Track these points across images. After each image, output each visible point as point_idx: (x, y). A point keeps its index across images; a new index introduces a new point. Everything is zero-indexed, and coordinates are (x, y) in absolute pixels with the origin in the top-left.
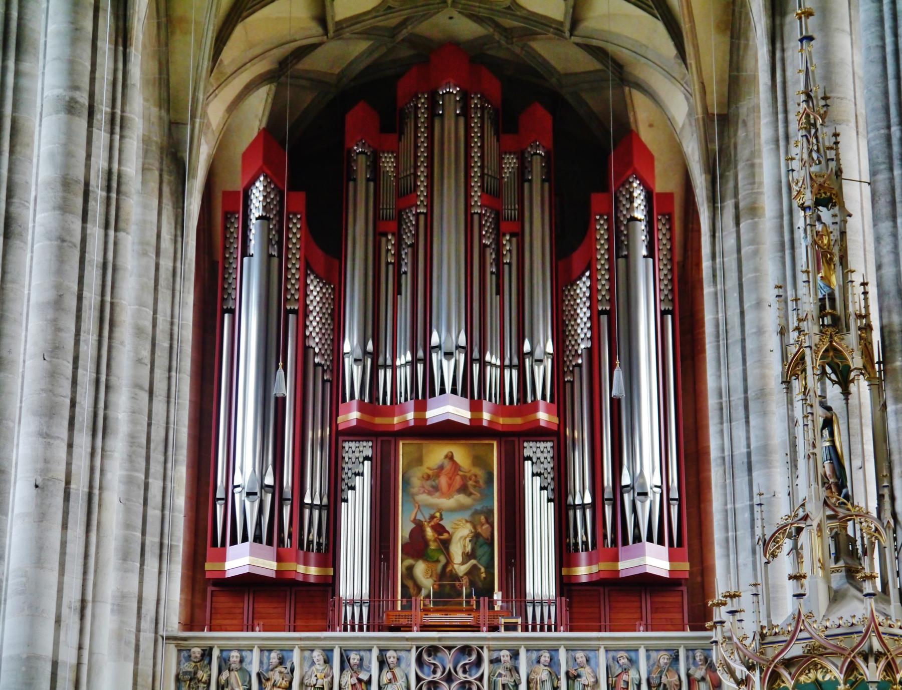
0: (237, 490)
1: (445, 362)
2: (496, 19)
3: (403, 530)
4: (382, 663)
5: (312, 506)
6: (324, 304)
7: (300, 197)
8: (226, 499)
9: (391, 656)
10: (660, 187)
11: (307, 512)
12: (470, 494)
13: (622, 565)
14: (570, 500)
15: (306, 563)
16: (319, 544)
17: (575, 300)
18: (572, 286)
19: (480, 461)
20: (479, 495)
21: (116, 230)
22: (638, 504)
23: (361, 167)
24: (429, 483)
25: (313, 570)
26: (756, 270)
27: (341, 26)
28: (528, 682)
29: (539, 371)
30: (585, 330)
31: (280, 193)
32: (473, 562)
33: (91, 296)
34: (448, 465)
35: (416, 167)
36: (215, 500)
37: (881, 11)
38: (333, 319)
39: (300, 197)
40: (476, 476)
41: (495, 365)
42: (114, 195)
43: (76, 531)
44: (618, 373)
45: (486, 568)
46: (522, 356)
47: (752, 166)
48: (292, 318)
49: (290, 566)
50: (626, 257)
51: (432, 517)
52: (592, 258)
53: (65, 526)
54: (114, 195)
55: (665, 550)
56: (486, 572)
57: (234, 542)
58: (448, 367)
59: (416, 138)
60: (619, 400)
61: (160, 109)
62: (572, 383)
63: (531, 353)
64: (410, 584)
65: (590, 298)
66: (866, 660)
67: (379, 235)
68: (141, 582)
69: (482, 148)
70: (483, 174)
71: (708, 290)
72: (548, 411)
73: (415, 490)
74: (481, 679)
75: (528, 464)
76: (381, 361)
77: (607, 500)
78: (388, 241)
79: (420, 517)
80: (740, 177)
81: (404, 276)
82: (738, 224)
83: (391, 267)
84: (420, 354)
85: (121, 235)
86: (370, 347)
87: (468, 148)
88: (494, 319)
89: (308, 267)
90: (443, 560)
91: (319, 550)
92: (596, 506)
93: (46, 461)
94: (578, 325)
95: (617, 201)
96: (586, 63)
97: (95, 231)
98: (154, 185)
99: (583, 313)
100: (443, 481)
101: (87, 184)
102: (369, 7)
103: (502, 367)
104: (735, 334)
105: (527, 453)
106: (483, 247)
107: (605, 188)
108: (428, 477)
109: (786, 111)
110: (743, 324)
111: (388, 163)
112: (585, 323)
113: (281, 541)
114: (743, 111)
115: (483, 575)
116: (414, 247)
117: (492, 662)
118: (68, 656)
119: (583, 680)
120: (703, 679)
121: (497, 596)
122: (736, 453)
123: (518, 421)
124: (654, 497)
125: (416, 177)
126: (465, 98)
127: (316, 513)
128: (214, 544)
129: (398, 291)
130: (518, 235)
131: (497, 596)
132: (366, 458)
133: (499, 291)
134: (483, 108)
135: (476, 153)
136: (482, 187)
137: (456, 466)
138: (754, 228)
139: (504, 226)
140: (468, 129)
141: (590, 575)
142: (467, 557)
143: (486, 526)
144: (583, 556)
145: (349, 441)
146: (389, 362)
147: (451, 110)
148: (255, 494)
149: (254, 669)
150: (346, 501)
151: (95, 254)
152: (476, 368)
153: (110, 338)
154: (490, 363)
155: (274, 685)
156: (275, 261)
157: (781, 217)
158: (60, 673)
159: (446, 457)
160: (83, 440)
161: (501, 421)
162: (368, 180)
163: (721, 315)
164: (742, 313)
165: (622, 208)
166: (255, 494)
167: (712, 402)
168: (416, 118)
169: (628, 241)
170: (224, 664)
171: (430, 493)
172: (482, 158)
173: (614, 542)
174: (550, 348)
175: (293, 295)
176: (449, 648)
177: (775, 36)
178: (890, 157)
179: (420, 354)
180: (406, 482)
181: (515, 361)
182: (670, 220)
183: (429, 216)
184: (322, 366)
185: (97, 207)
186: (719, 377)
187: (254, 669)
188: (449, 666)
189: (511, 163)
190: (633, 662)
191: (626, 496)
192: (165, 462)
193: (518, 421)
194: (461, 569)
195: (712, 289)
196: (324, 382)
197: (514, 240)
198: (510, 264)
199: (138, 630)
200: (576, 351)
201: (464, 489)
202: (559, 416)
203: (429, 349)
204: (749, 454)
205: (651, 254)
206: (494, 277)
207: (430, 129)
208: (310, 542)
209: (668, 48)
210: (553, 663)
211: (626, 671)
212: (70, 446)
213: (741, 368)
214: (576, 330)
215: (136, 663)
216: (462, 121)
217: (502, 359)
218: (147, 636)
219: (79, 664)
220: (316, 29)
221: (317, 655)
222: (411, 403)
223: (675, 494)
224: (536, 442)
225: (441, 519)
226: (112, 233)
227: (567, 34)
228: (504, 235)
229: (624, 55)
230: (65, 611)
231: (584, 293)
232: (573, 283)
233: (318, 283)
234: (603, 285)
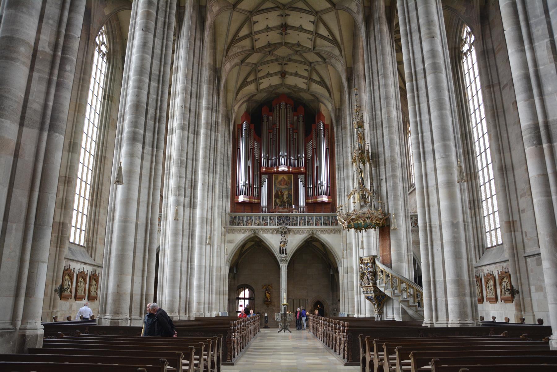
3: (274, 193)
4: (270, 219)
5: (256, 188)
7: (253, 125)
9: (272, 218)
10: (326, 123)
11: (255, 189)
12: (288, 185)
15: (255, 199)
19: (290, 178)
21: (217, 133)
22: (322, 187)
23: (265, 119)
25: (256, 201)
26: (346, 140)
27: (261, 90)
28: (300, 223)
29: (302, 160)
31: (249, 125)
33: (212, 146)
34: (283, 180)
36: (236, 187)
37: (371, 89)
39: (253, 125)
42: (217, 126)
43: (210, 193)
44: (318, 161)
46: (298, 157)
47: (345, 119)
49: (251, 200)
51: (280, 190)
53: (208, 192)
54: (217, 126)
55: (327, 196)
57: (240, 195)
58: (283, 160)
59: (276, 113)
60: (318, 166)
63: (300, 157)
64: (275, 203)
66: (367, 219)
68: (222, 203)
69: (290, 115)
71: (336, 144)
72: (303, 169)
73: (276, 185)
74: (290, 222)
76: (269, 158)
80: (342, 121)
82: (342, 131)
84: (277, 157)
85: (218, 134)
86: (267, 155)
89: (254, 139)
90: (282, 199)
93: (204, 179)
95: (317, 126)
96: (311, 98)
97: (213, 133)
98: (224, 123)
99: (310, 148)
100: (282, 183)
101: (211, 124)
103: (294, 160)
104: (341, 153)
105: (299, 177)
106: (290, 135)
107: (315, 123)
109: (352, 108)
110: (343, 151)
111: (271, 118)
113: (250, 195)
114: (343, 107)
116: (276, 135)
117: (292, 219)
118: (209, 217)
119: (310, 223)
120: (334, 222)
121: (294, 206)
123: (297, 170)
124: (325, 186)
126: (286, 104)
127: (257, 189)
128: (236, 195)
129: (273, 144)
130: (297, 133)
131: (294, 206)
134: (290, 107)
135: (288, 116)
136: (290, 123)
137: (285, 180)
138: (345, 132)
141: (312, 202)
142: (287, 198)
144: (310, 198)
147: (283, 107)
149: (245, 220)
151: (213, 138)
152: (289, 160)
153: (216, 154)
155: (249, 223)
156: (248, 138)
157: (351, 129)
158: (208, 221)
160: (211, 175)
161: (294, 170)
164: (343, 149)
167: (336, 167)
170: (239, 219)
171: (279, 185)
172: (290, 117)
173: (317, 195)
174: (304, 156)
176: (284, 216)
177: (349, 93)
178: (373, 118)
179: (277, 157)
181: (297, 158)
182: (328, 129)
183: (279, 129)
185: (213, 128)
186: (338, 162)
187: (245, 220)
188: (284, 220)
189: (296, 118)
190: (321, 219)
191: (319, 186)
192: (227, 179)
193: (297, 170)
194: (286, 200)
199: (222, 212)
201: (286, 184)
204: (344, 177)
205: (324, 136)
207: (279, 111)
208: (255, 195)
209: (327, 95)
210: (305, 219)
211: (319, 221)
212: (209, 176)
215: (222, 218)
216: (286, 109)
217: (294, 158)
218: (224, 214)
219: (211, 219)
220: (256, 91)
221: (257, 218)
222: (276, 167)
226: (216, 133)
227: (307, 91)
229: (319, 96)
230: (208, 208)
234: (314, 143)
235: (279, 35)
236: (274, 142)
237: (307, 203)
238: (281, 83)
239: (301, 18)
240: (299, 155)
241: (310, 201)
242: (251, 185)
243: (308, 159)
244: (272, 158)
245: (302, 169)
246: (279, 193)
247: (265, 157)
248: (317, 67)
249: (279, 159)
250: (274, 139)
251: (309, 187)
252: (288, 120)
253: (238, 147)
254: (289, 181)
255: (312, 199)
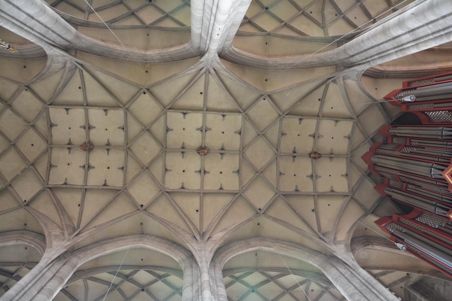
10: (401, 87)
18: (430, 119)
52: (418, 111)
61: (318, 256)
88: (431, 151)
89: (413, 219)
122: (411, 39)
139: (408, 144)
163: (376, 57)
195: (371, 62)
213: (385, 44)
234: (432, 106)
235: (225, 158)
238: (345, 159)
239: (184, 129)
248: (285, 106)
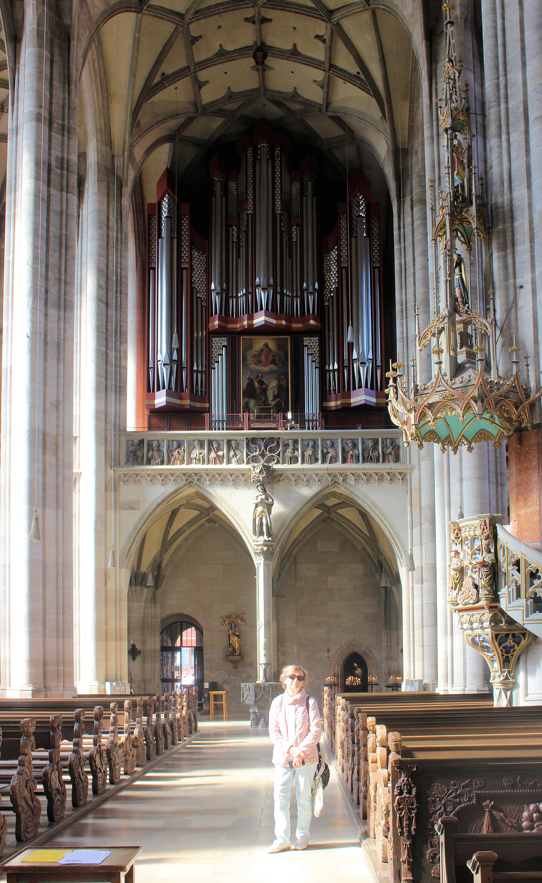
0: (159, 363)
1: (262, 294)
2: (288, 104)
3: (243, 384)
5: (197, 371)
6: (201, 265)
8: (154, 368)
11: (195, 374)
12: (276, 365)
13: (352, 400)
14: (327, 367)
16: (202, 391)
17: (330, 262)
19: (281, 346)
20: (281, 365)
22: (361, 368)
23: (218, 188)
24: (256, 358)
27: (205, 108)
30: (335, 278)
32: (278, 399)
34: (265, 350)
35: (247, 188)
36: (148, 368)
38: (206, 273)
40: (279, 355)
41: (288, 295)
45: (285, 403)
48: (185, 271)
50: (356, 237)
51: (258, 376)
55: (374, 392)
56: (285, 405)
57: (159, 390)
59: (247, 172)
62: (328, 306)
63: (307, 289)
65: (337, 261)
67: (228, 226)
69: (281, 177)
70: (281, 192)
73: (248, 363)
75: (306, 348)
76: (230, 295)
77: (346, 367)
78: (233, 229)
79: (251, 377)
81: (241, 248)
83: (235, 244)
84: (250, 290)
87: (274, 178)
89: (192, 245)
91: (202, 394)
92: (340, 371)
94: (332, 275)
95: (351, 207)
99: (334, 268)
100: (263, 358)
102: (220, 97)
106: (282, 232)
108: (256, 356)
112: (335, 274)
115: (284, 406)
116: (247, 232)
121: (289, 416)
125: (247, 193)
127: (199, 375)
129: (238, 256)
130: (300, 226)
131: (289, 416)
132: (224, 346)
133: (291, 256)
134: (281, 155)
135: (278, 181)
137: (270, 350)
140: (274, 167)
141: (336, 406)
142: (275, 397)
143: (285, 381)
144: (333, 396)
145: (215, 337)
146: (234, 295)
148: (168, 364)
150: (215, 368)
154: (286, 294)
159: (264, 345)
162: (222, 196)
165: (353, 211)
166: (168, 364)
168: (247, 161)
169: (357, 228)
171: (256, 364)
172: (281, 183)
175: (185, 259)
179: (250, 290)
180: (245, 359)
181: (299, 294)
183: (254, 215)
184: (201, 298)
189: (296, 186)
191: (355, 364)
196: (202, 306)
197: (298, 228)
198: (296, 242)
200: (330, 289)
201: (273, 362)
202: (321, 323)
203: (255, 286)
205: (368, 235)
206: (287, 248)
214: (330, 278)
217: (292, 294)
222: (246, 316)
223: (379, 363)
224: (310, 337)
225: (262, 377)
228: (293, 226)
231: (334, 258)
232: (329, 252)
233: (198, 253)
236: (243, 251)
237: (324, 410)
240: (305, 285)
241: (332, 404)
242: (184, 364)
243: (328, 295)
244: (237, 294)
245: (312, 322)
246: (256, 384)
247: (219, 289)
249: (254, 294)
250: (243, 244)
251: (331, 368)
252: (278, 191)
253: (153, 265)
254: (279, 352)
255: (336, 400)
